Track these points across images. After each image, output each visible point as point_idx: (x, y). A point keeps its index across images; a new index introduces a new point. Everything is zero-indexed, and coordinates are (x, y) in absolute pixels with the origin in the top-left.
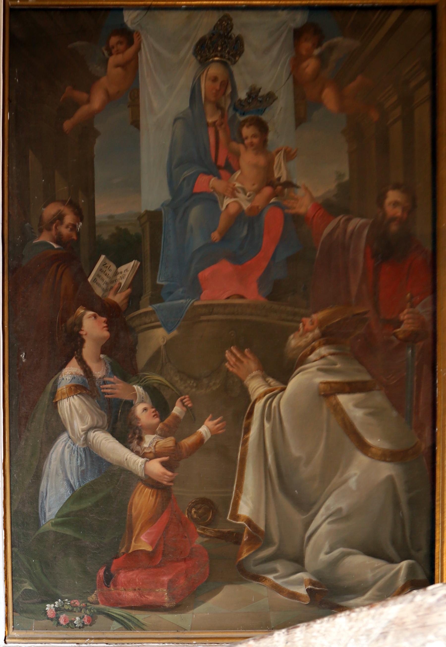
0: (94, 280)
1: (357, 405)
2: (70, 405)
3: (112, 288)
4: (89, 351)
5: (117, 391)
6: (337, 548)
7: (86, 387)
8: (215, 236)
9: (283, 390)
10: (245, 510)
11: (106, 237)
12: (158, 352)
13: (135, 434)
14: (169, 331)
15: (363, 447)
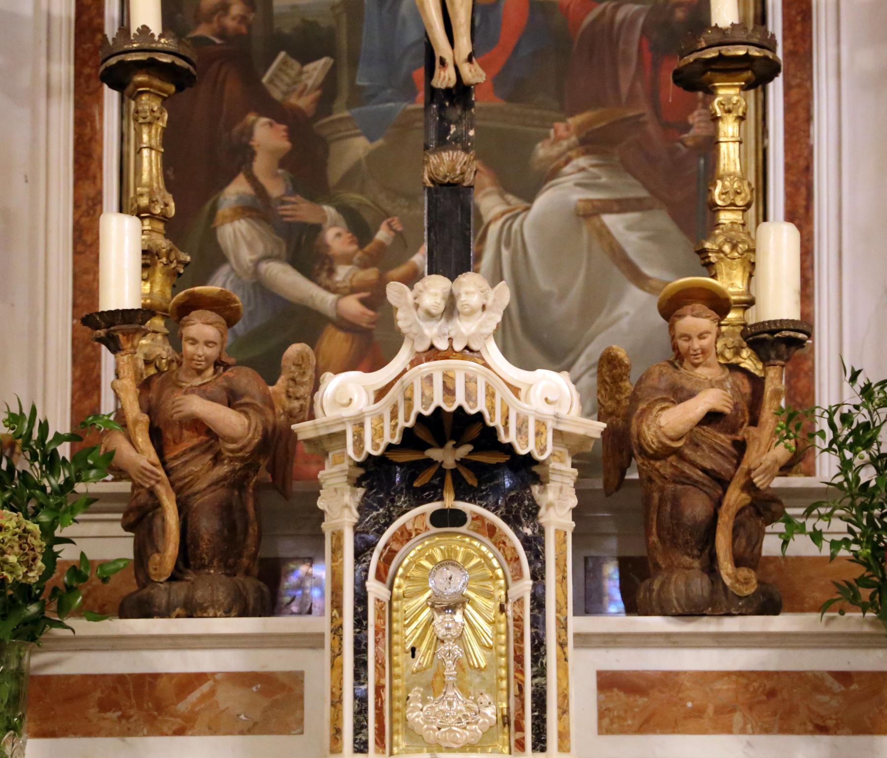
0: (271, 81)
1: (630, 228)
2: (235, 232)
3: (294, 90)
4: (261, 166)
5: (298, 213)
7: (259, 208)
9: (527, 209)
11: (287, 31)
13: (323, 264)
14: (371, 139)
15: (638, 278)
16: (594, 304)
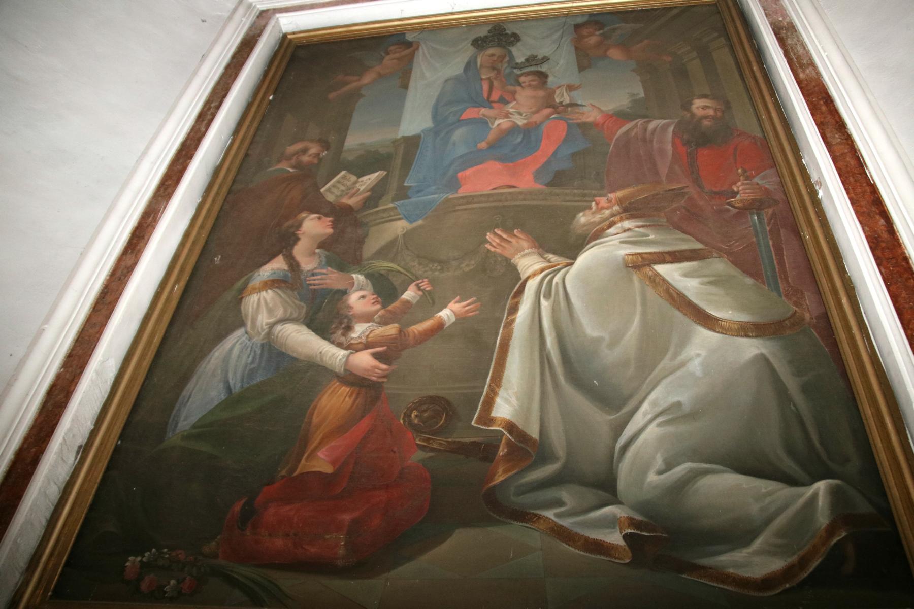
0: (329, 190)
1: (687, 275)
2: (259, 300)
5: (328, 281)
6: (679, 464)
8: (483, 145)
9: (572, 264)
10: (504, 409)
12: (393, 242)
13: (341, 323)
16: (654, 351)
